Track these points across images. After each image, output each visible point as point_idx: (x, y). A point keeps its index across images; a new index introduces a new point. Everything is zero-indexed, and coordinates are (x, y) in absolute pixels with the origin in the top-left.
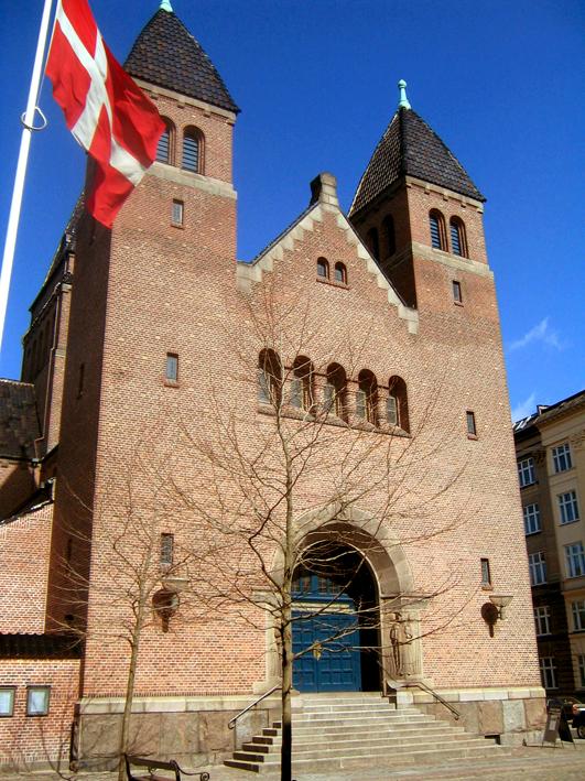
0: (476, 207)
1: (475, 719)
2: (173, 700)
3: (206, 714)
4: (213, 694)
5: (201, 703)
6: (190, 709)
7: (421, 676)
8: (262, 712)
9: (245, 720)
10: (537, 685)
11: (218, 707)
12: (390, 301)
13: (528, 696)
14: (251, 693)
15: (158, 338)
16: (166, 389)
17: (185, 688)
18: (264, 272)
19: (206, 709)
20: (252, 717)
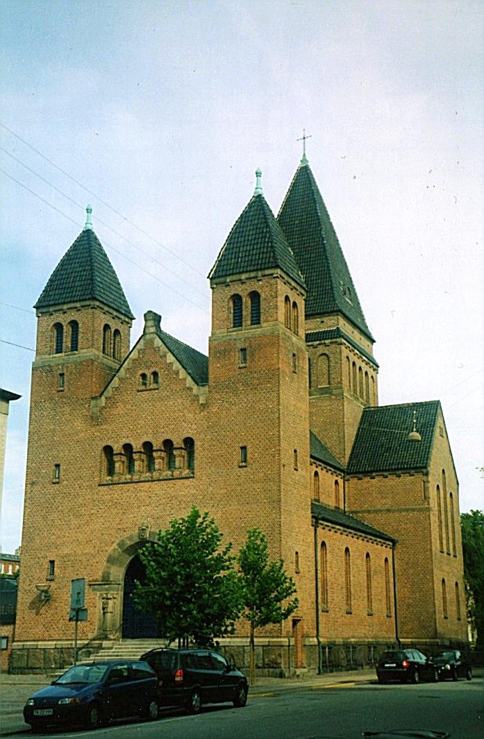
0: (272, 274)
2: (50, 643)
12: (187, 385)
17: (56, 637)
18: (106, 398)
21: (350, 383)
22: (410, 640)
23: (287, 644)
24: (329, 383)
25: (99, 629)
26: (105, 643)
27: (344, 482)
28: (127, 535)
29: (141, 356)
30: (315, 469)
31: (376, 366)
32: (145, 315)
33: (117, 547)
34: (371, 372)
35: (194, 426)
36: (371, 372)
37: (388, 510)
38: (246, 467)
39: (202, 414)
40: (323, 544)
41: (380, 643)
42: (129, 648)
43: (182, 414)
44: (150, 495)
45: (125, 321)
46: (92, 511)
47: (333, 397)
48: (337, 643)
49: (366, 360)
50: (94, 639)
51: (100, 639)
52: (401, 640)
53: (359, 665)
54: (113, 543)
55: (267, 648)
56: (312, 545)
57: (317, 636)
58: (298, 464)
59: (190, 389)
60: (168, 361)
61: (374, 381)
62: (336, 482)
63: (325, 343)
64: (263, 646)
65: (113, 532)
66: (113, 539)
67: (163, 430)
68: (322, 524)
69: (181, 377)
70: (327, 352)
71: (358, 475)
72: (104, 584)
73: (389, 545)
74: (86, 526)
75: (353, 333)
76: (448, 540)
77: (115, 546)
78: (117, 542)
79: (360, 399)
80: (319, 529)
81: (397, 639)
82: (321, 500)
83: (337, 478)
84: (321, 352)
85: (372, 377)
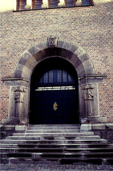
7: (99, 116)
25: (12, 115)
26: (18, 128)
28: (36, 43)
33: (28, 52)
44: (56, 17)
46: (7, 29)
50: (8, 124)
51: (12, 124)
54: (24, 49)
65: (25, 42)
72: (16, 80)
77: (26, 51)
78: (29, 48)
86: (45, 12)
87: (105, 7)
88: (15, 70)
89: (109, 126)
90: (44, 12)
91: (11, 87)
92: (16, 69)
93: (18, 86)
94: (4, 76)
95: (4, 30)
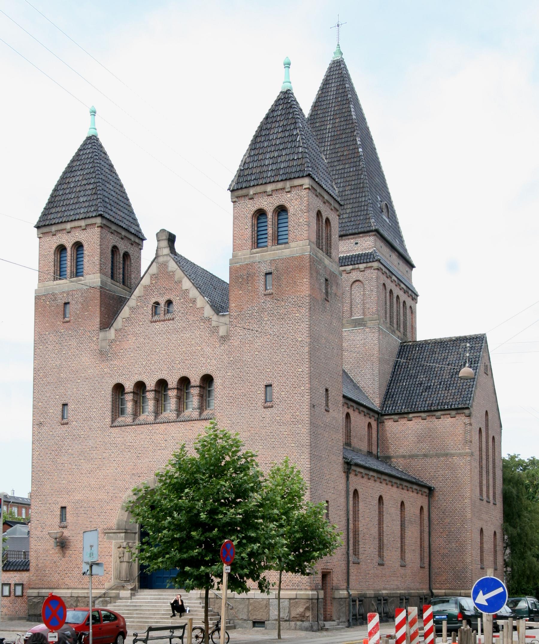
1: (246, 610)
3: (80, 599)
4: (85, 589)
5: (78, 593)
6: (73, 595)
8: (108, 599)
9: (99, 602)
10: (306, 589)
11: (86, 595)
12: (206, 315)
13: (294, 597)
14: (104, 588)
15: (58, 397)
16: (62, 426)
19: (80, 596)
20: (102, 601)
21: (386, 314)
22: (443, 591)
23: (316, 597)
24: (364, 314)
27: (378, 425)
29: (154, 282)
30: (346, 410)
31: (414, 296)
32: (157, 235)
34: (409, 302)
35: (214, 362)
36: (409, 302)
37: (425, 456)
38: (272, 407)
39: (222, 347)
40: (356, 492)
41: (413, 595)
42: (148, 599)
43: (199, 348)
45: (135, 242)
46: (104, 455)
47: (367, 330)
48: (368, 596)
49: (405, 288)
52: (434, 591)
53: (390, 618)
55: (294, 601)
56: (343, 493)
57: (348, 588)
58: (330, 404)
59: (209, 319)
60: (184, 288)
61: (412, 313)
62: (369, 425)
63: (358, 268)
64: (290, 599)
66: (127, 485)
67: (179, 366)
68: (355, 471)
69: (198, 306)
70: (361, 279)
71: (392, 417)
72: (119, 533)
73: (425, 492)
74: (98, 471)
75: (390, 256)
76: (488, 487)
77: (130, 492)
79: (397, 332)
80: (352, 476)
81: (430, 589)
82: (353, 444)
83: (370, 420)
84: (355, 278)
85: (411, 307)
86: (151, 428)
87: (229, 422)
88: (117, 518)
89: (218, 593)
90: (151, 428)
91: (113, 541)
92: (119, 517)
93: (121, 541)
94: (105, 526)
95: (100, 457)
